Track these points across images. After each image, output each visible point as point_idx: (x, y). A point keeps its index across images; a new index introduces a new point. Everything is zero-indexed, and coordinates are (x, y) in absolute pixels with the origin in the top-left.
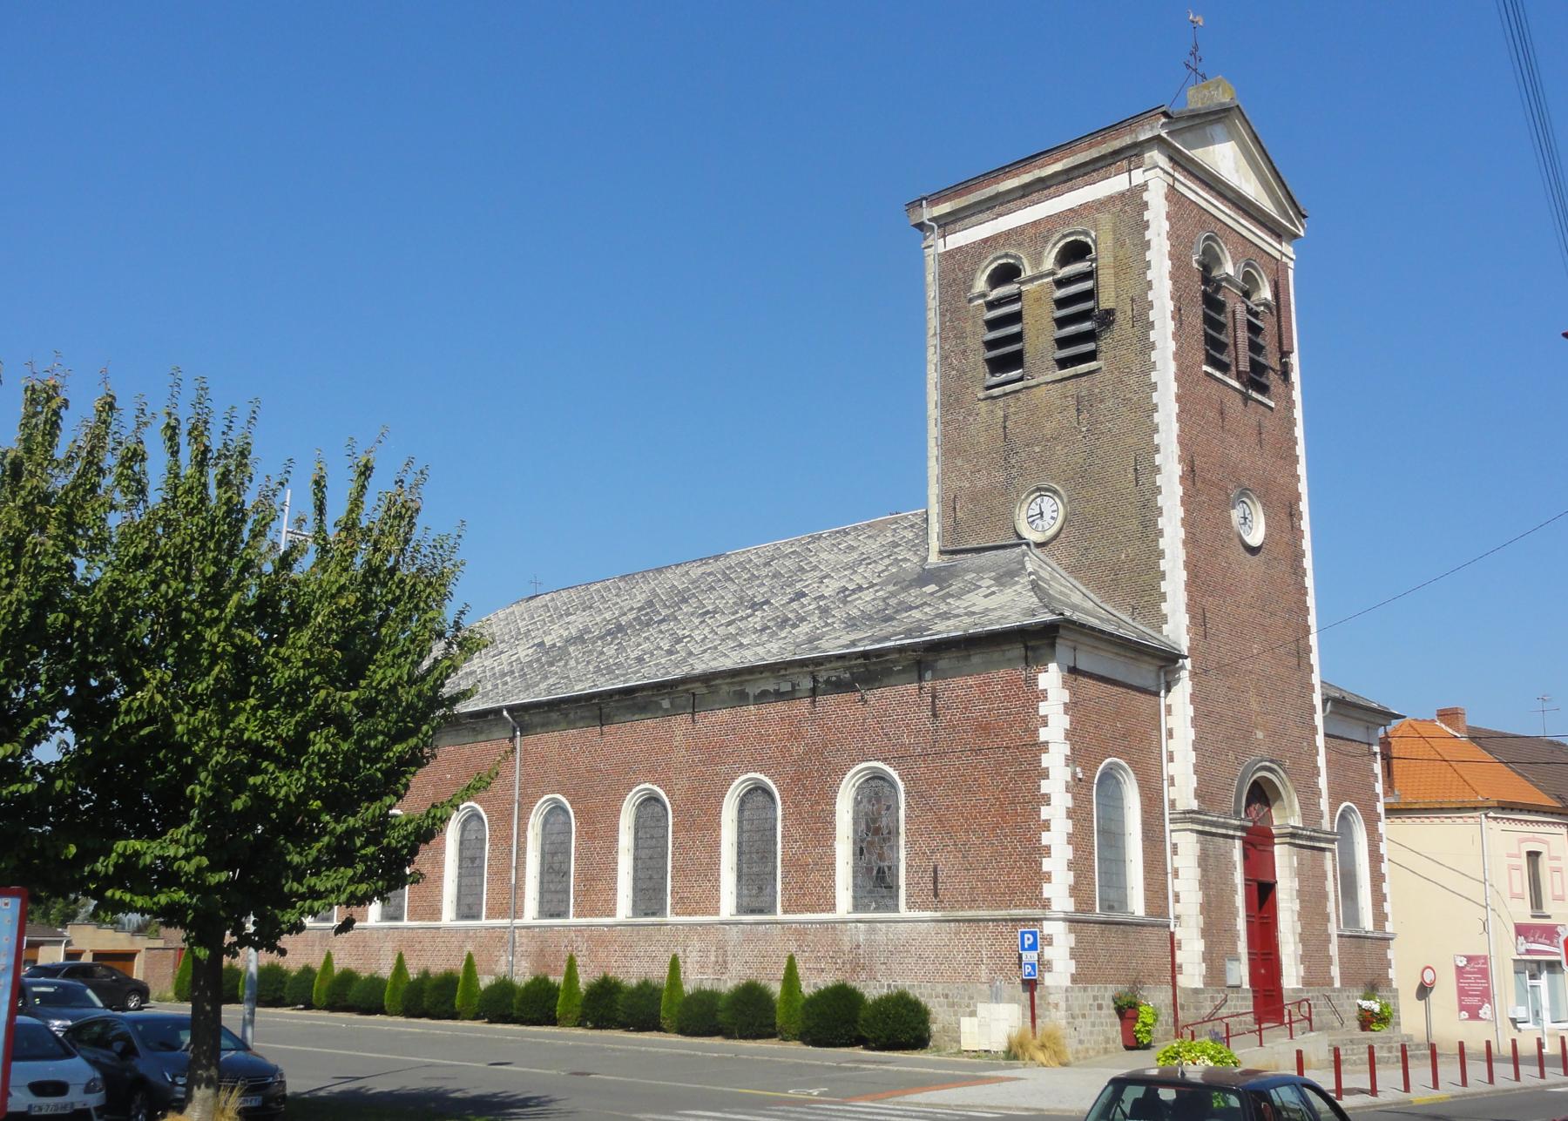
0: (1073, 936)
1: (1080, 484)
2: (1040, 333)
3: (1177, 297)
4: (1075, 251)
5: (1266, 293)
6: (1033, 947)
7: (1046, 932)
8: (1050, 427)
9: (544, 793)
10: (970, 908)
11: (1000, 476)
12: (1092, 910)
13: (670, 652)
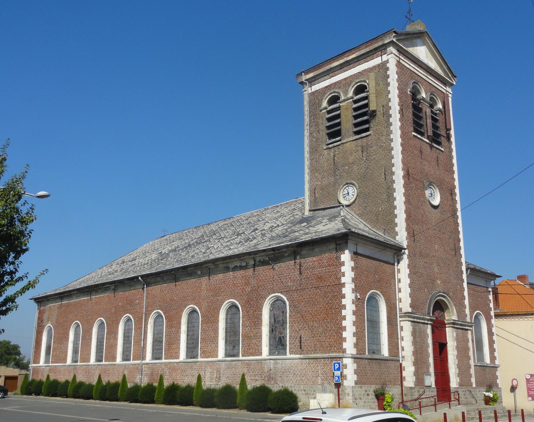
0: (356, 365)
1: (363, 181)
2: (347, 122)
3: (401, 104)
4: (361, 89)
5: (440, 106)
6: (339, 369)
7: (344, 363)
8: (351, 159)
9: (154, 310)
10: (314, 353)
11: (332, 179)
12: (365, 354)
13: (204, 253)
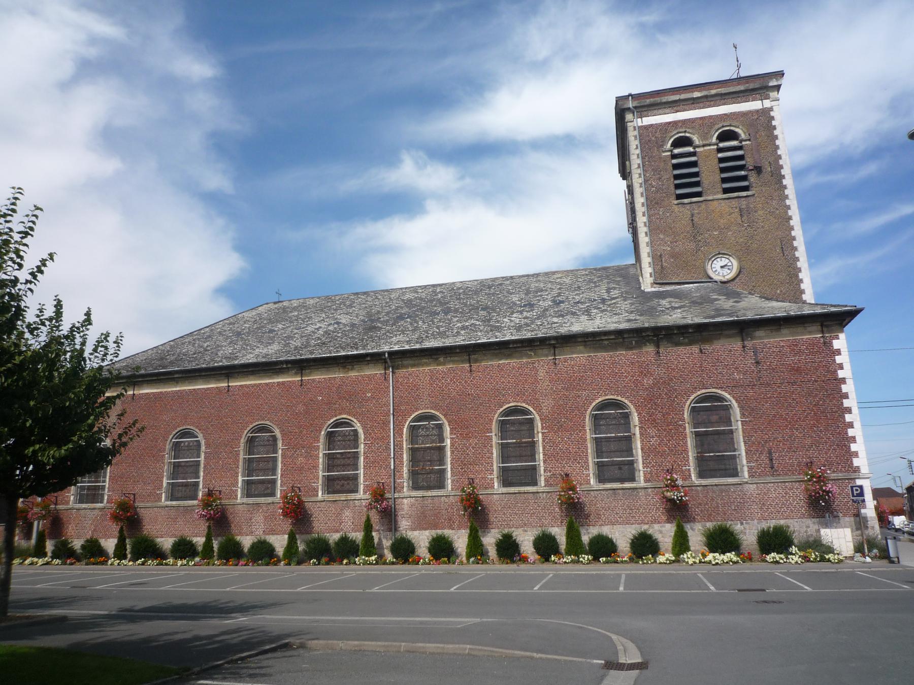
2: (710, 174)
11: (692, 245)
